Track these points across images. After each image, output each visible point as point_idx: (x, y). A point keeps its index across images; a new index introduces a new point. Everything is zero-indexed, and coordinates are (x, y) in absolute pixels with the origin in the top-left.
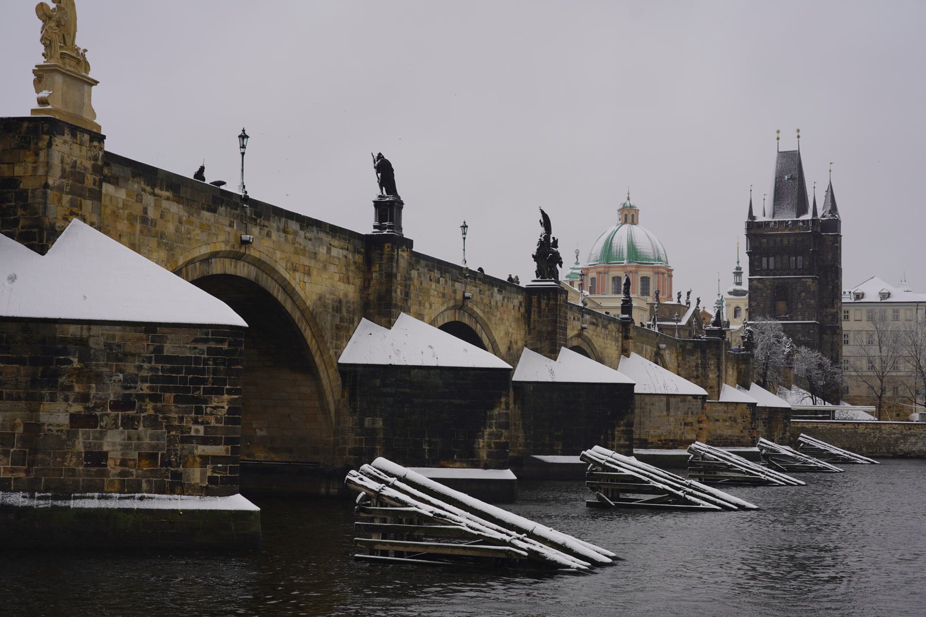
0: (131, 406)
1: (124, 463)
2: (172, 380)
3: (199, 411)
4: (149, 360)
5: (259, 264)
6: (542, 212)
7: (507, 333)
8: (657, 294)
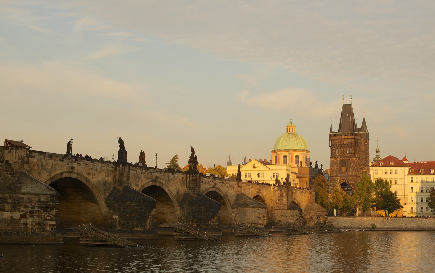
0: (33, 213)
1: (32, 225)
2: (42, 207)
3: (49, 214)
5: (78, 174)
6: (191, 147)
7: (176, 188)
8: (301, 162)
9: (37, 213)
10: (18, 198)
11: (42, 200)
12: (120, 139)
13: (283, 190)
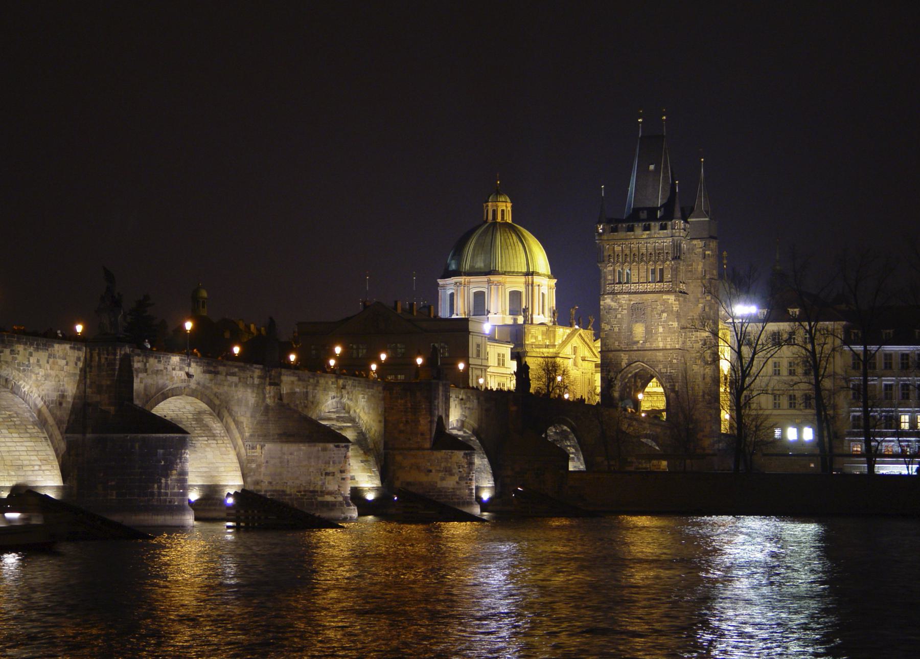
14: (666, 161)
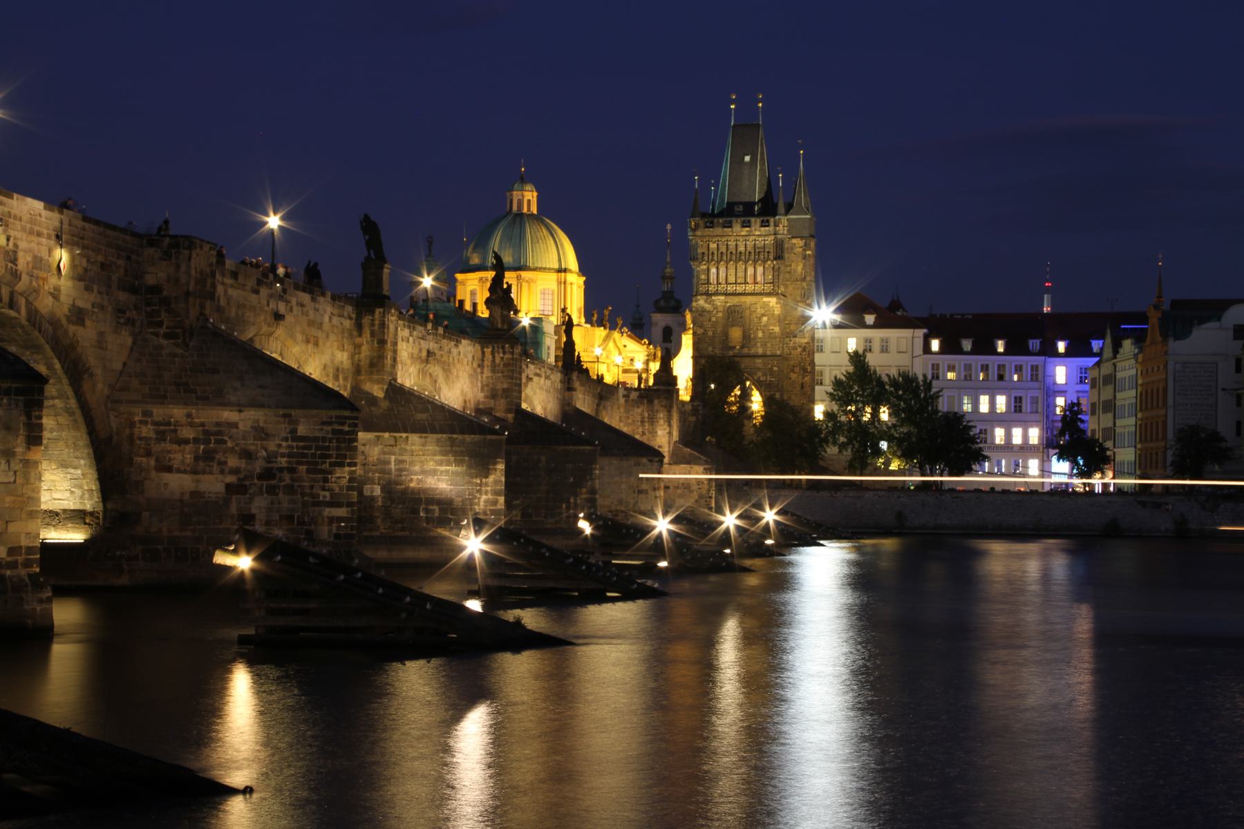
0: (273, 477)
1: (268, 523)
2: (304, 455)
3: (326, 480)
4: (286, 439)
9: (287, 477)
10: (218, 424)
11: (302, 430)
12: (366, 218)
13: (656, 402)
14: (762, 153)
